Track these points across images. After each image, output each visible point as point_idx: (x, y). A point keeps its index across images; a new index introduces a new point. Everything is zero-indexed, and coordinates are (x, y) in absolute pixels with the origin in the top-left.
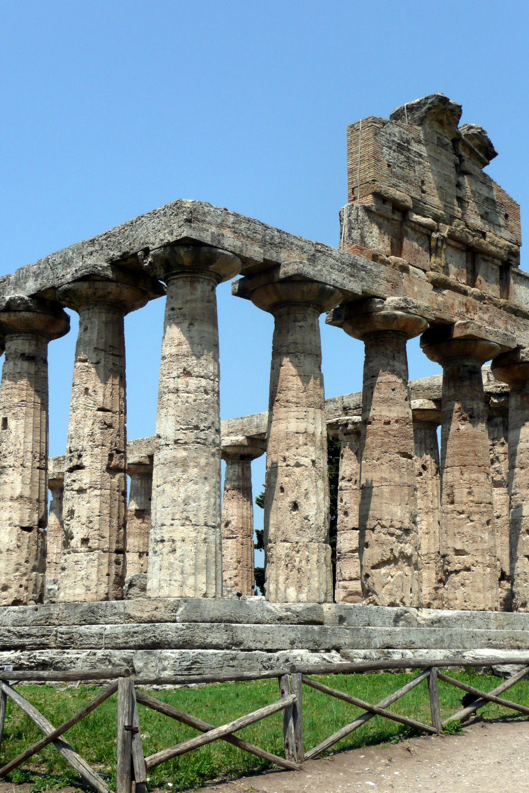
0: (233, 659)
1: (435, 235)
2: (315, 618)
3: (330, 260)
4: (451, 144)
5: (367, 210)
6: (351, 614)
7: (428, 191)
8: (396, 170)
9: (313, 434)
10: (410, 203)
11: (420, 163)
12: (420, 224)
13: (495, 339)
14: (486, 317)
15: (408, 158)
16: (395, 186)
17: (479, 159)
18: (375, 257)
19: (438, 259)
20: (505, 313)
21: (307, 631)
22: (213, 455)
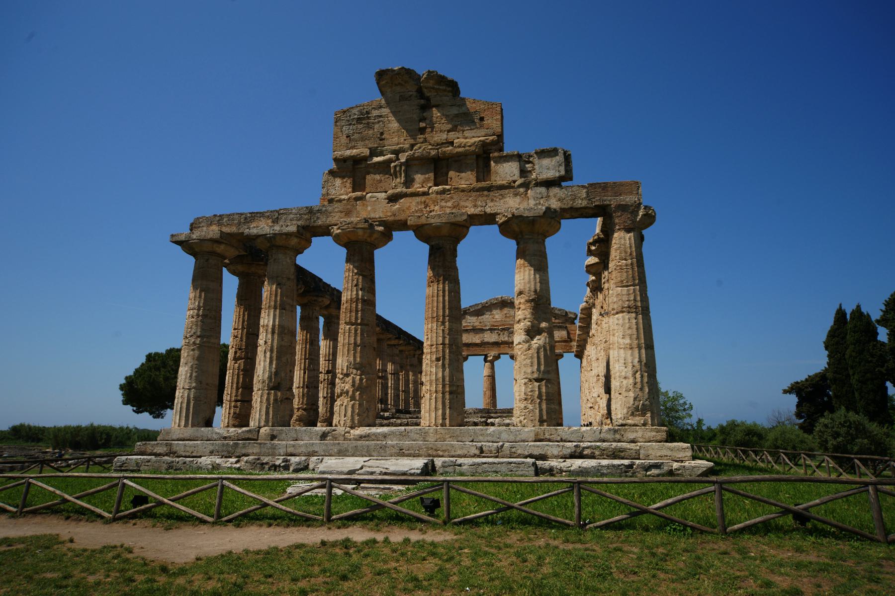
0: (149, 461)
1: (393, 165)
2: (250, 436)
3: (292, 216)
4: (415, 94)
5: (332, 173)
6: (281, 434)
7: (388, 137)
8: (356, 136)
9: (267, 326)
10: (367, 152)
11: (379, 122)
12: (379, 163)
13: (439, 221)
14: (449, 204)
15: (368, 123)
16: (353, 148)
17: (445, 90)
18: (331, 201)
19: (398, 180)
20: (474, 194)
21: (223, 445)
22: (193, 350)
